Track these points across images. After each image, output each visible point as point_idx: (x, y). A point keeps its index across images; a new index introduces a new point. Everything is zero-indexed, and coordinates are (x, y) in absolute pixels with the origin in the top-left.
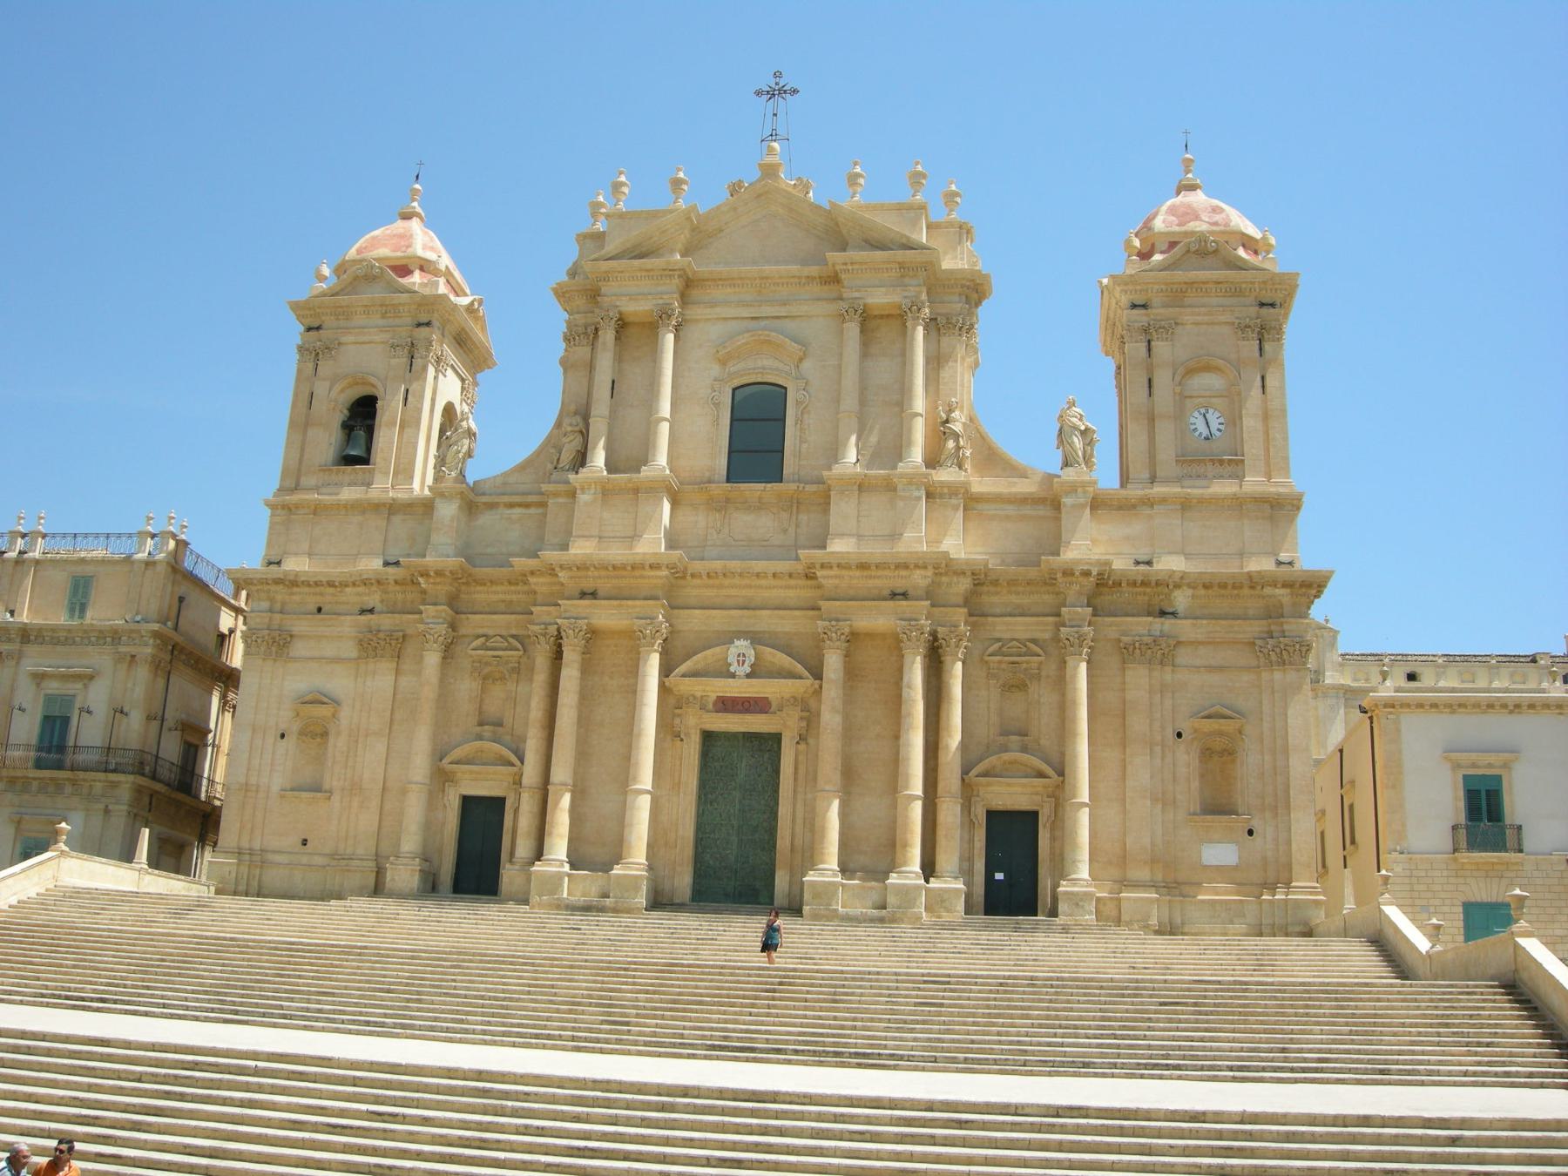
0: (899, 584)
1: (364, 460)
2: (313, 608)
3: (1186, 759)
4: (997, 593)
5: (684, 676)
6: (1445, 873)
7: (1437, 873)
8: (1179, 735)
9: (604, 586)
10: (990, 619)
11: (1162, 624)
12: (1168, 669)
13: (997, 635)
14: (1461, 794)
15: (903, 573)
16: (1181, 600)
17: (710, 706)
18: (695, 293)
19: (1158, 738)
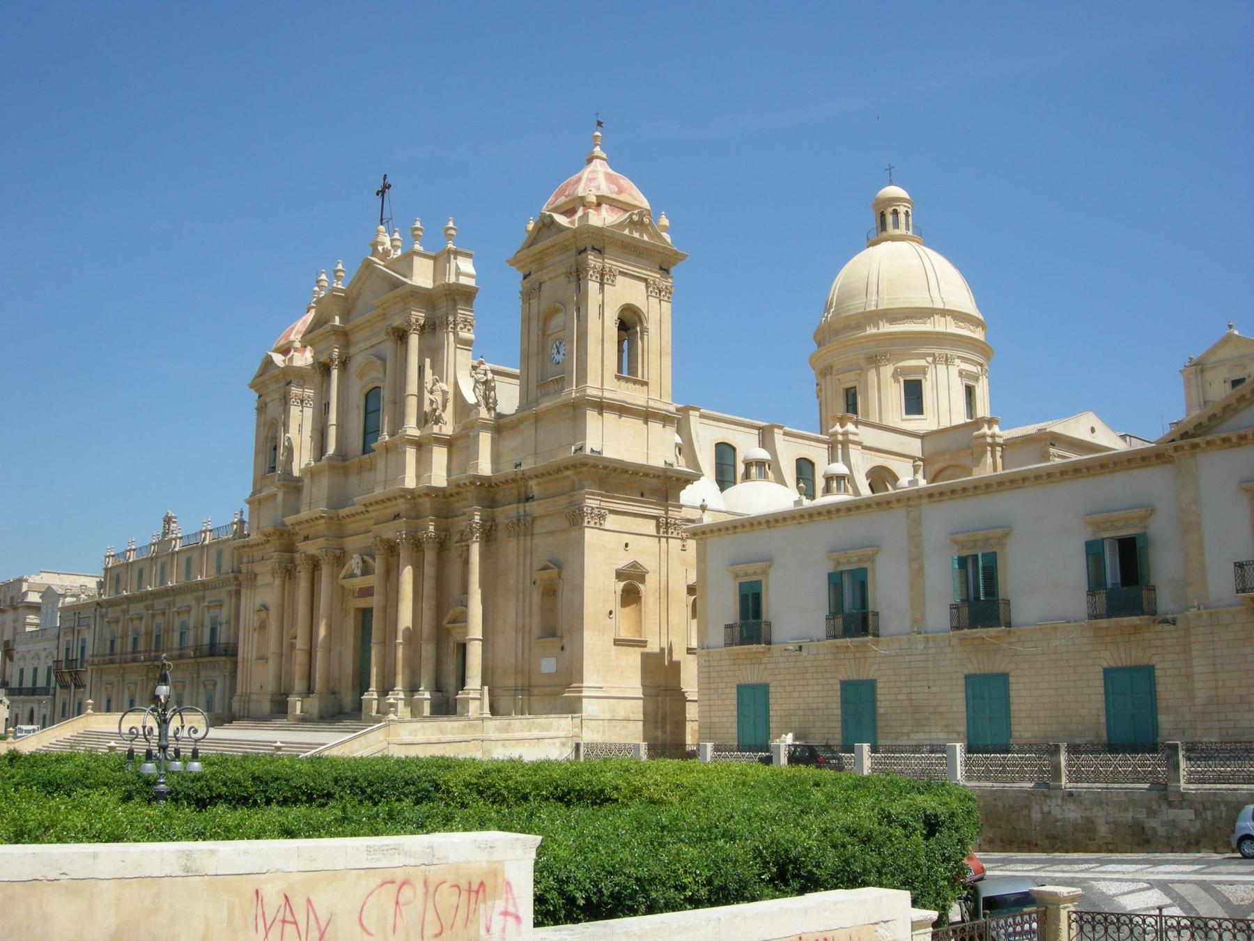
0: (395, 510)
1: (273, 469)
2: (260, 558)
3: (536, 598)
4: (458, 501)
5: (344, 578)
6: (728, 663)
7: (723, 663)
8: (534, 583)
9: (310, 532)
10: (456, 519)
11: (525, 507)
12: (529, 538)
13: (461, 528)
14: (738, 597)
15: (394, 502)
16: (535, 487)
17: (357, 595)
18: (353, 338)
19: (521, 586)
